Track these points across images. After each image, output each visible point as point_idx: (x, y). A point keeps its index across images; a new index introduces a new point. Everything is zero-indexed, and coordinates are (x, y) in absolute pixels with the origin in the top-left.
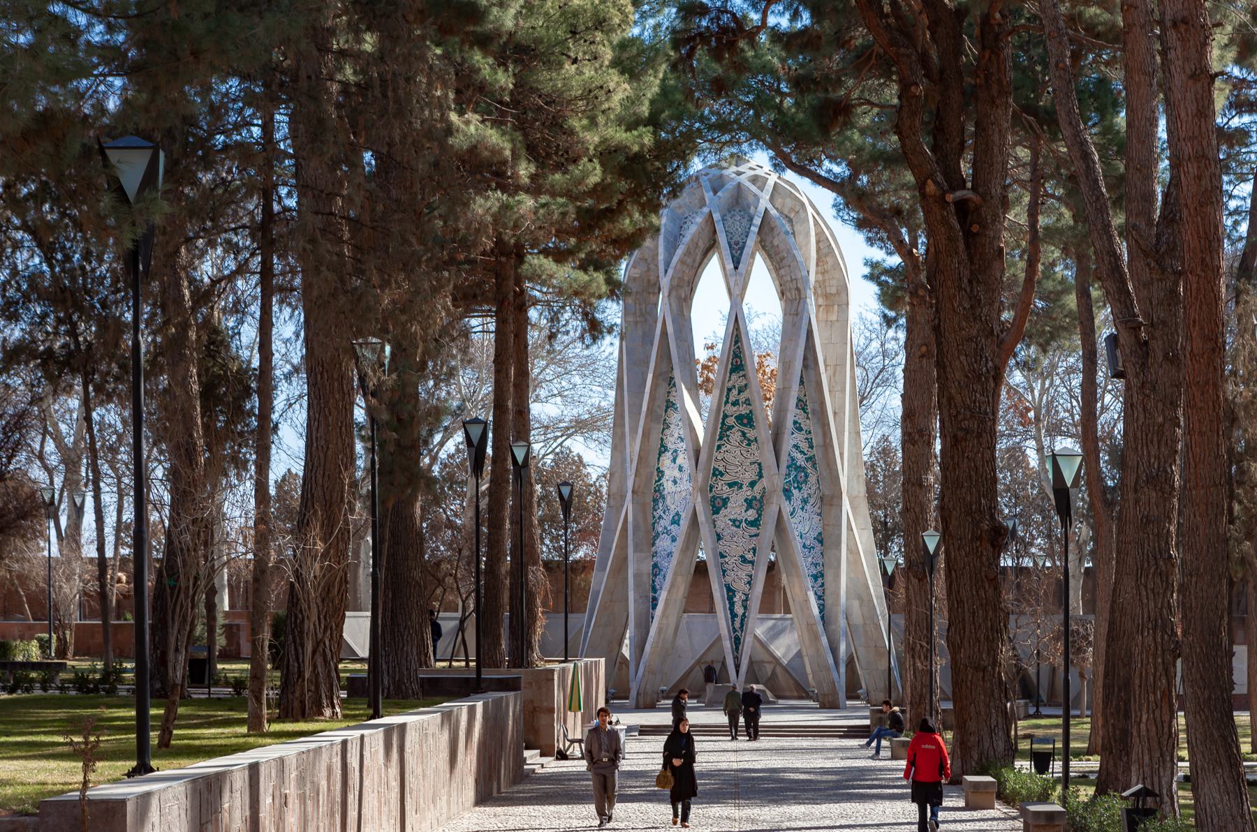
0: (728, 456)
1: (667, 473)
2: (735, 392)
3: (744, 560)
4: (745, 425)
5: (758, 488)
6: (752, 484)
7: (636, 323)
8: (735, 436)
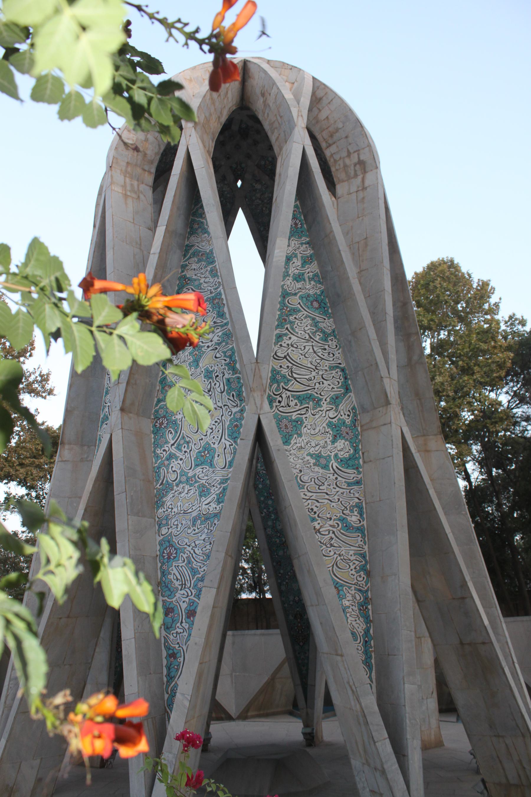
0: (295, 355)
2: (297, 262)
3: (348, 527)
6: (336, 400)
7: (126, 196)
8: (303, 326)
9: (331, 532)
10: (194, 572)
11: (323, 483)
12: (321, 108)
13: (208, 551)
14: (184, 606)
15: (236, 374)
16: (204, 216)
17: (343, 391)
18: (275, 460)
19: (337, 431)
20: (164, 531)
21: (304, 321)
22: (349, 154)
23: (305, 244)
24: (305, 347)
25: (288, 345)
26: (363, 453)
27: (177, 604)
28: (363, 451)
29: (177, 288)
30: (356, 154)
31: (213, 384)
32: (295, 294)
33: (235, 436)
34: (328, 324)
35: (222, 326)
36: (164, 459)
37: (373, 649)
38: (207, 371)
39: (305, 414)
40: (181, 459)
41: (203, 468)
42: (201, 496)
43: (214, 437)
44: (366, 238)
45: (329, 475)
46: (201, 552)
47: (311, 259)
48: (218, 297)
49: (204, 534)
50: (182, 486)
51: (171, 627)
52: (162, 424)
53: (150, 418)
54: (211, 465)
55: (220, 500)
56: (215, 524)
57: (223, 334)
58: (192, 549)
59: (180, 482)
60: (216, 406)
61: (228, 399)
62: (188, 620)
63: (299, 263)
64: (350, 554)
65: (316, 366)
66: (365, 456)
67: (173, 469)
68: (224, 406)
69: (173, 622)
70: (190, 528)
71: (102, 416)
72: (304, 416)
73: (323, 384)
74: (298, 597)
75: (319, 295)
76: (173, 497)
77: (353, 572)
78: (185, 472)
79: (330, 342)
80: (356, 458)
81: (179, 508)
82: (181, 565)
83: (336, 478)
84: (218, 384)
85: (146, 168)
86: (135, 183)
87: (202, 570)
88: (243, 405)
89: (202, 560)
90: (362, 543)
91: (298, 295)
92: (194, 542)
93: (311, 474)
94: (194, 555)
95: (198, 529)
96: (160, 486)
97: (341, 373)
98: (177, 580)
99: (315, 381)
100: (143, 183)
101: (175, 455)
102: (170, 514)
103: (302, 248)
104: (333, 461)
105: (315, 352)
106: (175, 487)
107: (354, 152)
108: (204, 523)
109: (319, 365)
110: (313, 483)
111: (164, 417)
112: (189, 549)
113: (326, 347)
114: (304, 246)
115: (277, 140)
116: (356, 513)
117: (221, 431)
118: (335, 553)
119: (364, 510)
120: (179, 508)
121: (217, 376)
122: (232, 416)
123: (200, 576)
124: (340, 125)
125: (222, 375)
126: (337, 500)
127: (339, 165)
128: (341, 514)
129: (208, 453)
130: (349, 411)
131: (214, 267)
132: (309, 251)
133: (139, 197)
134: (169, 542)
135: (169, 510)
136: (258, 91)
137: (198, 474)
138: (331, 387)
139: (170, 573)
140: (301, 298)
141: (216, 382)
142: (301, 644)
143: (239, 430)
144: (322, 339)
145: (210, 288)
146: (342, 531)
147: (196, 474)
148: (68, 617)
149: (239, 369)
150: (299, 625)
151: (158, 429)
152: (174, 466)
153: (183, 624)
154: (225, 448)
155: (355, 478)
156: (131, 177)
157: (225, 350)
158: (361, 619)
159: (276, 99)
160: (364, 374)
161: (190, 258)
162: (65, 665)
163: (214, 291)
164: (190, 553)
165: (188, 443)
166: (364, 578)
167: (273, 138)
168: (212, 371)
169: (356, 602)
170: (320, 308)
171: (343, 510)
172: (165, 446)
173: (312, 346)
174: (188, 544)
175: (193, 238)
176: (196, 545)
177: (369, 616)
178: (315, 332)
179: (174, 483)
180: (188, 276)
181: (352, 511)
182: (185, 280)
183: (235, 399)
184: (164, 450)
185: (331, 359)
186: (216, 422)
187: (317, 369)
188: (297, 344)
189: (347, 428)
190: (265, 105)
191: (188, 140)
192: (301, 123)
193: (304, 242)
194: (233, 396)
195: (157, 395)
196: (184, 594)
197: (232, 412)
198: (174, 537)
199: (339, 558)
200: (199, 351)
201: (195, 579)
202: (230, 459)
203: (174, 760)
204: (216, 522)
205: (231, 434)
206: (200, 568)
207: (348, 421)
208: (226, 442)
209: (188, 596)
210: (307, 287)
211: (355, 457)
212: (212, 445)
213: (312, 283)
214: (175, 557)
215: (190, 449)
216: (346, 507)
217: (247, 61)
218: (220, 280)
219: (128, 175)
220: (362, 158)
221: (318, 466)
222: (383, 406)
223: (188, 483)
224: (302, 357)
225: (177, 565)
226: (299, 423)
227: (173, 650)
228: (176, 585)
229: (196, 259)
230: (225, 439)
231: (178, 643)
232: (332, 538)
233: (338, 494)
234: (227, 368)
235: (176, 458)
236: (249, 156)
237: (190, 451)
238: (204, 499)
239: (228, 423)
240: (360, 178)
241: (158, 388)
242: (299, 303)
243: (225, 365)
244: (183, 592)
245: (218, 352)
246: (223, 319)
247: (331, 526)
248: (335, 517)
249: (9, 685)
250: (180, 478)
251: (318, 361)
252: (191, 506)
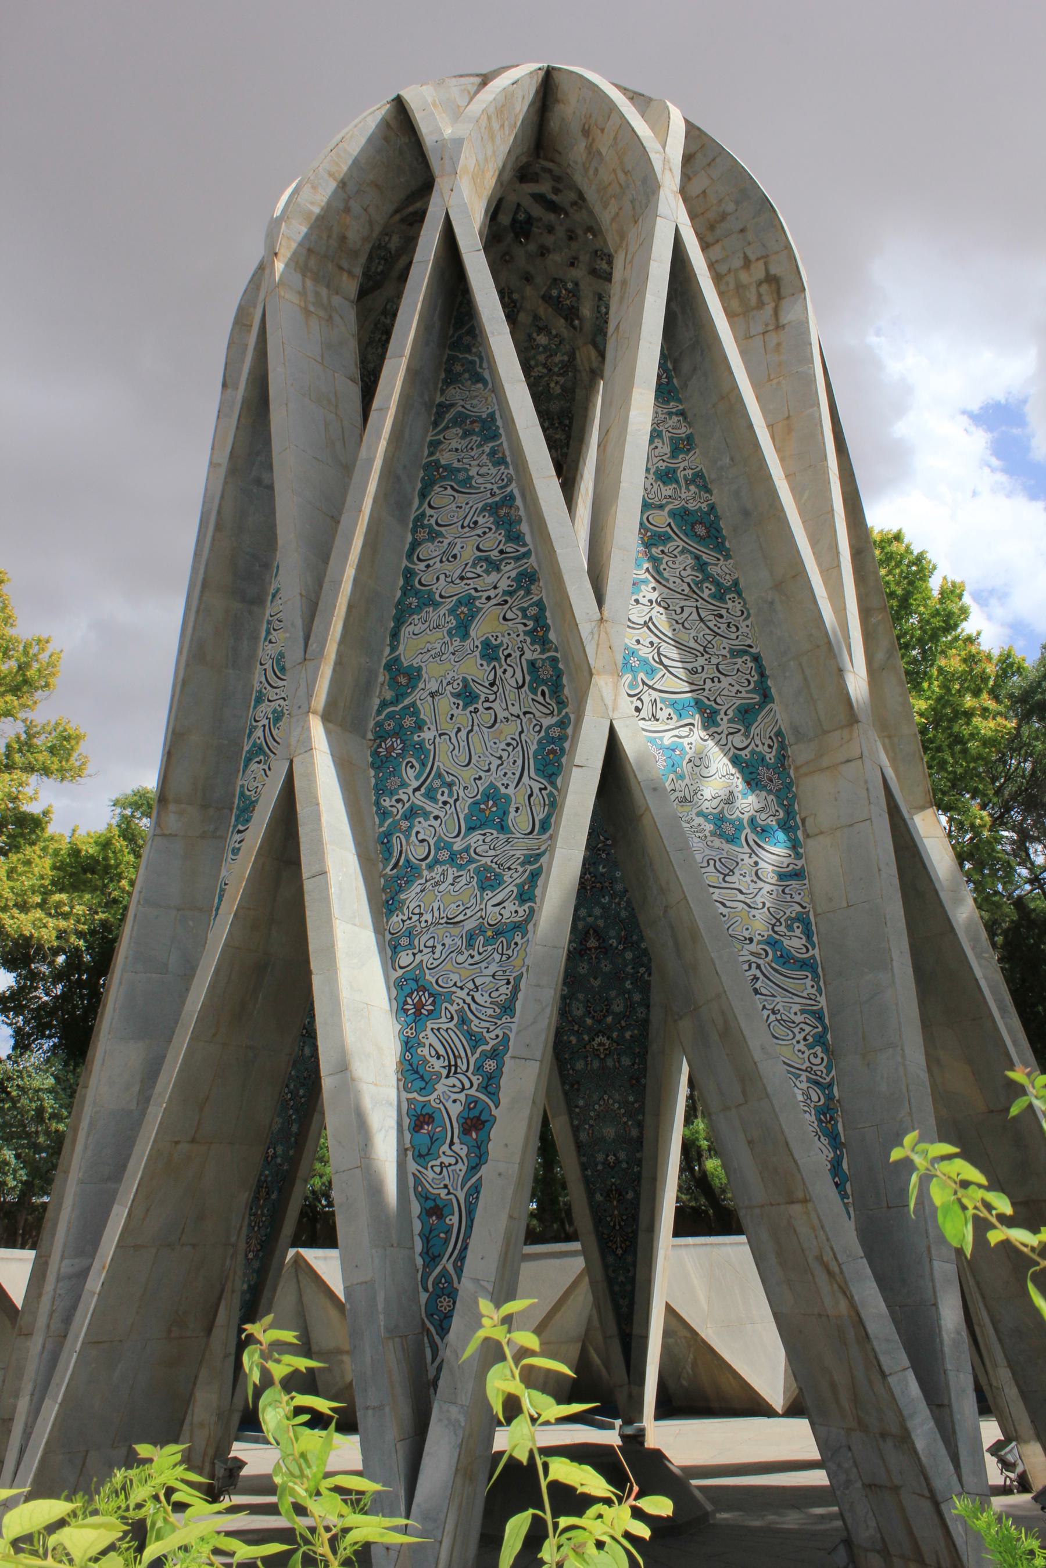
1: (433, 675)
3: (786, 959)
4: (700, 539)
5: (762, 726)
7: (307, 313)
9: (754, 966)
10: (475, 1040)
11: (732, 871)
12: (691, 175)
13: (503, 997)
14: (455, 1110)
15: (549, 651)
16: (474, 350)
17: (757, 698)
18: (648, 808)
19: (751, 773)
20: (405, 958)
21: (680, 559)
22: (747, 263)
23: (676, 414)
24: (682, 608)
25: (651, 601)
26: (803, 821)
27: (441, 1106)
28: (803, 815)
29: (420, 485)
30: (761, 263)
31: (499, 672)
32: (661, 507)
33: (550, 772)
34: (724, 568)
35: (517, 559)
36: (398, 817)
37: (850, 1200)
38: (487, 644)
39: (687, 736)
40: (436, 818)
41: (484, 835)
42: (483, 889)
43: (505, 774)
44: (788, 417)
45: (741, 856)
46: (489, 1000)
47: (688, 444)
48: (509, 503)
49: (494, 964)
50: (440, 870)
51: (428, 1154)
52: (392, 748)
53: (364, 737)
54: (503, 828)
55: (524, 897)
56: (516, 944)
57: (520, 574)
58: (468, 994)
59: (437, 862)
60: (506, 714)
61: (533, 700)
62: (467, 1137)
63: (667, 449)
64: (793, 1011)
65: (705, 647)
66: (807, 823)
67: (420, 837)
68: (525, 713)
69: (432, 1144)
70: (462, 953)
71: (246, 748)
72: (686, 741)
73: (719, 682)
74: (615, 1155)
75: (706, 513)
76: (422, 891)
77: (801, 1046)
78: (446, 842)
79: (730, 604)
80: (791, 827)
81: (436, 914)
82: (445, 1026)
83: (756, 863)
84: (510, 671)
85: (345, 264)
86: (324, 292)
87: (493, 1035)
88: (563, 713)
89: (490, 1016)
90: (813, 991)
91: (667, 509)
92: (473, 980)
93: (707, 852)
94: (473, 1006)
95: (480, 954)
96: (392, 870)
97: (752, 664)
98: (438, 1058)
99: (704, 675)
100: (337, 293)
101: (423, 808)
102: (415, 926)
103: (670, 423)
104: (748, 830)
105: (701, 620)
106: (425, 873)
107: (758, 259)
108: (491, 941)
109: (710, 645)
110: (711, 868)
111: (396, 734)
112: (462, 994)
113: (723, 612)
114: (675, 419)
115: (613, 220)
116: (798, 932)
117: (519, 762)
118: (764, 1007)
119: (814, 928)
120: (436, 914)
121: (509, 655)
122: (543, 734)
123: (488, 1048)
124: (730, 207)
125: (518, 653)
126: (761, 905)
127: (727, 284)
128: (771, 932)
129: (495, 804)
130: (770, 738)
131: (498, 446)
132: (684, 429)
133: (331, 317)
134: (417, 981)
135: (415, 918)
136: (575, 127)
137: (474, 846)
138: (734, 690)
139: (421, 1044)
140: (673, 514)
141: (505, 667)
142: (619, 1252)
143: (558, 761)
144: (713, 596)
145: (489, 486)
146: (773, 965)
147: (469, 846)
148: (193, 1141)
149: (555, 641)
150: (616, 1212)
151: (384, 759)
152: (421, 831)
153: (457, 1147)
154: (531, 796)
155: (791, 866)
156: (316, 279)
157: (525, 605)
158: (822, 1138)
159: (615, 138)
160: (800, 665)
161: (447, 428)
162: (183, 1245)
163: (498, 492)
164: (464, 1002)
165: (450, 785)
166: (822, 1059)
167: (605, 217)
168: (498, 647)
169: (812, 1105)
170: (709, 537)
171: (773, 926)
172: (401, 792)
173: (697, 608)
174: (459, 984)
175: (453, 391)
176: (477, 987)
177: (838, 1134)
178: (702, 582)
179: (423, 864)
180: (443, 462)
181: (790, 928)
182: (437, 470)
183: (548, 700)
184: (398, 801)
185: (734, 636)
186: (508, 745)
187: (707, 653)
188: (668, 601)
189: (768, 769)
190: (590, 153)
191: (446, 199)
192: (670, 181)
193: (674, 410)
194: (543, 694)
195: (380, 692)
196: (454, 1086)
197: (541, 727)
198: (427, 971)
199: (772, 1018)
200: (471, 606)
201: (477, 1055)
202: (541, 816)
203: (462, 1419)
204: (517, 939)
205: (542, 768)
206: (488, 1032)
207: (770, 757)
208: (533, 782)
209: (463, 1089)
210: (683, 496)
211: (787, 825)
212: (503, 790)
213: (693, 488)
214: (430, 1012)
215: (455, 797)
216: (778, 920)
217: (554, 68)
218: (511, 471)
219: (309, 274)
220: (772, 271)
221: (720, 836)
222: (842, 728)
223: (454, 864)
224: (677, 627)
225: (436, 1026)
226: (678, 752)
227: (434, 1200)
228: (437, 1069)
229: (460, 432)
230: (530, 778)
231: (446, 1186)
232: (756, 979)
233: (760, 893)
234: (528, 640)
235: (426, 815)
236: (528, 278)
237: (456, 801)
238: (491, 895)
239: (534, 747)
240: (769, 309)
241: (381, 679)
242: (669, 525)
243: (526, 633)
244: (452, 1081)
245: (510, 608)
246: (521, 546)
247: (752, 954)
248: (760, 938)
249: (55, 1290)
250: (436, 853)
251: (709, 638)
252: (461, 908)
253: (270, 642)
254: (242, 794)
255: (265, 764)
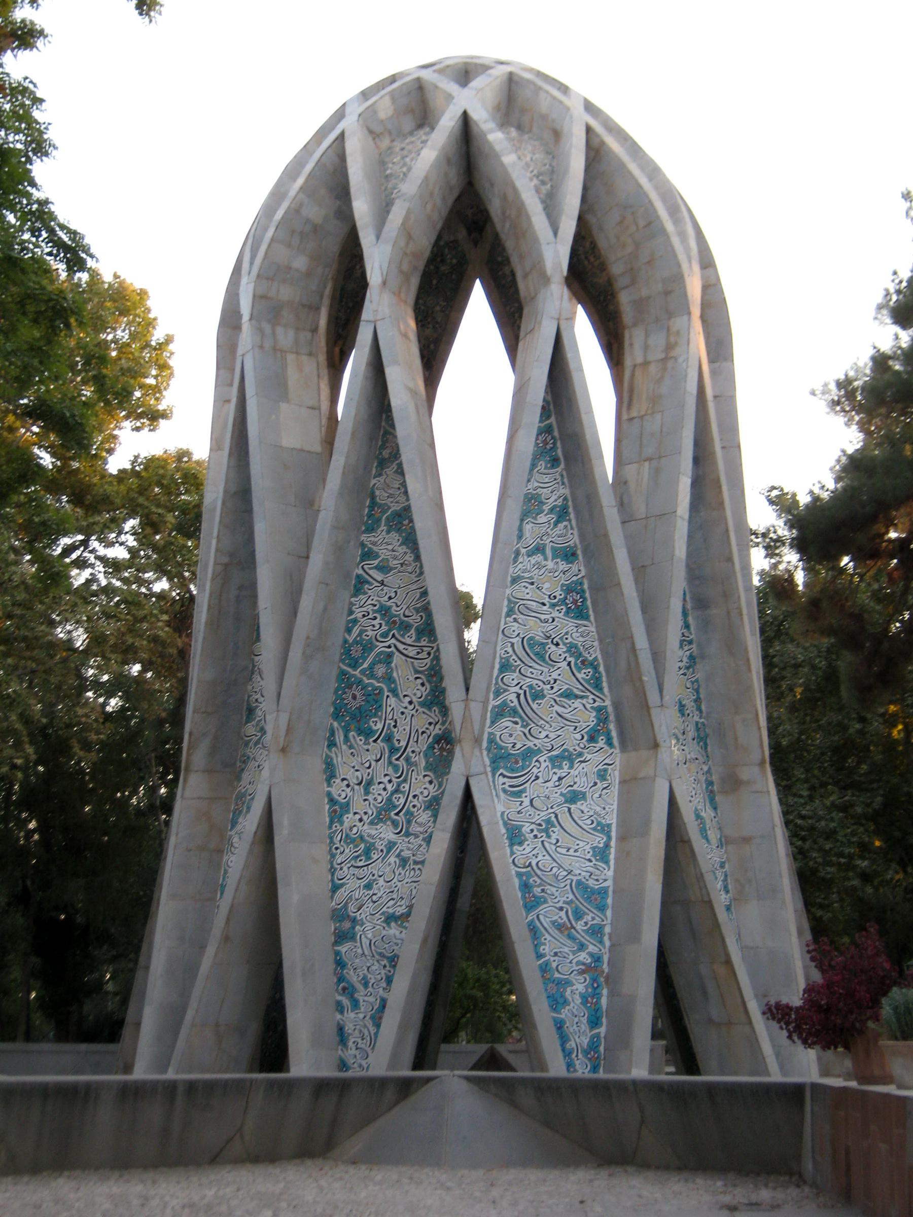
253: (515, 620)
254: (491, 741)
255: (525, 727)
